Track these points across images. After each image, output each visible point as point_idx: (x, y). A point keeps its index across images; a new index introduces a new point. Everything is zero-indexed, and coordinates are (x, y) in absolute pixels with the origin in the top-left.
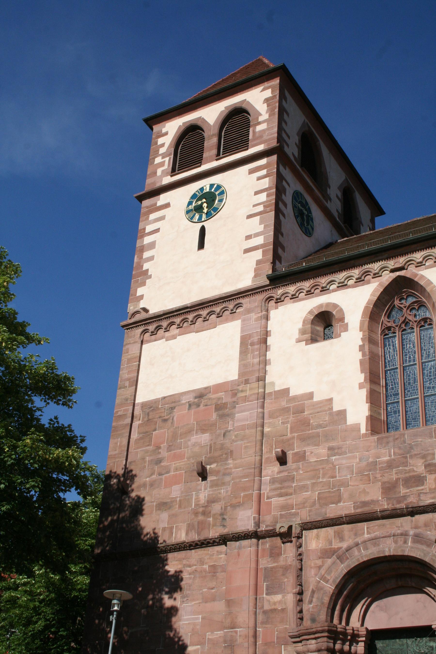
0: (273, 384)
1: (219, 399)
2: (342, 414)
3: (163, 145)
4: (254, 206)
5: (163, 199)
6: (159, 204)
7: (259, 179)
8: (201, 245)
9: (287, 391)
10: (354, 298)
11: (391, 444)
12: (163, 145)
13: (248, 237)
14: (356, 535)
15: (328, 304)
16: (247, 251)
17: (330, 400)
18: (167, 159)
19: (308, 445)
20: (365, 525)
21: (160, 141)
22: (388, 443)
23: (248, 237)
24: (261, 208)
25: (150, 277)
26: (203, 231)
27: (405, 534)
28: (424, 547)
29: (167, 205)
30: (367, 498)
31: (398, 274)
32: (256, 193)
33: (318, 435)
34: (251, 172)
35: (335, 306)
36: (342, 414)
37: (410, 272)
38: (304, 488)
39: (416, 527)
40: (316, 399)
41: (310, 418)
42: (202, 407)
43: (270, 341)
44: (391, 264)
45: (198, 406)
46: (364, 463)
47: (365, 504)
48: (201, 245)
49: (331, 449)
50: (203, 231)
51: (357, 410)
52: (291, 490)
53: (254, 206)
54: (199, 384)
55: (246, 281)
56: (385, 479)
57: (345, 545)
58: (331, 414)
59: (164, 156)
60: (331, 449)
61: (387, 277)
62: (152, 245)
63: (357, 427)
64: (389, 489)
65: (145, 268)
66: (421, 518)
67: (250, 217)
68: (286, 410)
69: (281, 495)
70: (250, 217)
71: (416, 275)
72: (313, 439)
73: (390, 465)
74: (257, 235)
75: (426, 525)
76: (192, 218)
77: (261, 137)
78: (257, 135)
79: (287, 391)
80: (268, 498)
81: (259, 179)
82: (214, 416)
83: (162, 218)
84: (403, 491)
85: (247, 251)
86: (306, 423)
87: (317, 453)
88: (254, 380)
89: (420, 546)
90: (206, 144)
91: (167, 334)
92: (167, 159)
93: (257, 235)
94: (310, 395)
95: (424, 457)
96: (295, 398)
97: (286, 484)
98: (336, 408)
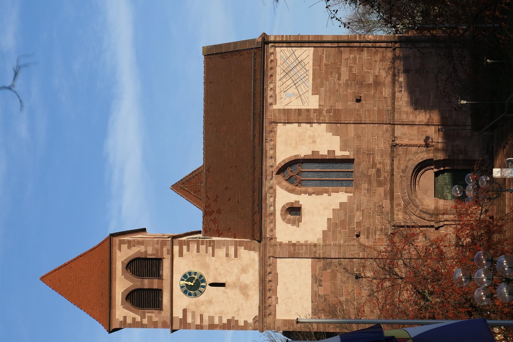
0: (318, 239)
1: (320, 269)
2: (341, 204)
3: (134, 319)
4: (207, 252)
5: (178, 314)
6: (181, 316)
8: (223, 285)
9: (324, 232)
10: (282, 197)
11: (361, 182)
12: (134, 319)
14: (399, 198)
15: (282, 211)
18: (147, 314)
19: (354, 220)
20: (395, 194)
21: (129, 321)
22: (359, 184)
23: (227, 255)
24: (210, 249)
25: (233, 317)
26: (212, 285)
27: (401, 177)
28: (408, 169)
30: (383, 194)
31: (274, 175)
33: (350, 216)
34: (181, 254)
35: (284, 206)
36: (341, 204)
37: (275, 170)
38: (374, 222)
39: (399, 172)
40: (331, 217)
42: (323, 279)
43: (294, 242)
44: (269, 177)
45: (321, 280)
46: (367, 195)
47: (385, 195)
48: (223, 285)
49: (357, 210)
50: (212, 285)
51: (341, 197)
52: (374, 229)
53: (207, 252)
54: (309, 280)
55: (255, 256)
56: (376, 185)
57: (402, 203)
58: (340, 209)
60: (357, 210)
62: (211, 318)
63: (349, 198)
64: (380, 184)
65: (226, 322)
66: (396, 170)
67: (213, 255)
68: (334, 231)
69: (375, 234)
70: (213, 255)
71: (278, 166)
72: (351, 218)
73: (370, 183)
74: (227, 250)
75: (398, 168)
76: (201, 292)
77: (157, 250)
78: (154, 252)
79: (324, 232)
80: (376, 240)
81: (188, 250)
82: (329, 271)
83: (193, 313)
84: (382, 178)
85: (236, 256)
86: (343, 223)
87: (358, 217)
88: (315, 248)
89: (407, 171)
91: (274, 303)
92: (147, 314)
93: (227, 250)
94: (329, 220)
95: (368, 169)
96: (328, 227)
97: (371, 231)
98: (338, 207)
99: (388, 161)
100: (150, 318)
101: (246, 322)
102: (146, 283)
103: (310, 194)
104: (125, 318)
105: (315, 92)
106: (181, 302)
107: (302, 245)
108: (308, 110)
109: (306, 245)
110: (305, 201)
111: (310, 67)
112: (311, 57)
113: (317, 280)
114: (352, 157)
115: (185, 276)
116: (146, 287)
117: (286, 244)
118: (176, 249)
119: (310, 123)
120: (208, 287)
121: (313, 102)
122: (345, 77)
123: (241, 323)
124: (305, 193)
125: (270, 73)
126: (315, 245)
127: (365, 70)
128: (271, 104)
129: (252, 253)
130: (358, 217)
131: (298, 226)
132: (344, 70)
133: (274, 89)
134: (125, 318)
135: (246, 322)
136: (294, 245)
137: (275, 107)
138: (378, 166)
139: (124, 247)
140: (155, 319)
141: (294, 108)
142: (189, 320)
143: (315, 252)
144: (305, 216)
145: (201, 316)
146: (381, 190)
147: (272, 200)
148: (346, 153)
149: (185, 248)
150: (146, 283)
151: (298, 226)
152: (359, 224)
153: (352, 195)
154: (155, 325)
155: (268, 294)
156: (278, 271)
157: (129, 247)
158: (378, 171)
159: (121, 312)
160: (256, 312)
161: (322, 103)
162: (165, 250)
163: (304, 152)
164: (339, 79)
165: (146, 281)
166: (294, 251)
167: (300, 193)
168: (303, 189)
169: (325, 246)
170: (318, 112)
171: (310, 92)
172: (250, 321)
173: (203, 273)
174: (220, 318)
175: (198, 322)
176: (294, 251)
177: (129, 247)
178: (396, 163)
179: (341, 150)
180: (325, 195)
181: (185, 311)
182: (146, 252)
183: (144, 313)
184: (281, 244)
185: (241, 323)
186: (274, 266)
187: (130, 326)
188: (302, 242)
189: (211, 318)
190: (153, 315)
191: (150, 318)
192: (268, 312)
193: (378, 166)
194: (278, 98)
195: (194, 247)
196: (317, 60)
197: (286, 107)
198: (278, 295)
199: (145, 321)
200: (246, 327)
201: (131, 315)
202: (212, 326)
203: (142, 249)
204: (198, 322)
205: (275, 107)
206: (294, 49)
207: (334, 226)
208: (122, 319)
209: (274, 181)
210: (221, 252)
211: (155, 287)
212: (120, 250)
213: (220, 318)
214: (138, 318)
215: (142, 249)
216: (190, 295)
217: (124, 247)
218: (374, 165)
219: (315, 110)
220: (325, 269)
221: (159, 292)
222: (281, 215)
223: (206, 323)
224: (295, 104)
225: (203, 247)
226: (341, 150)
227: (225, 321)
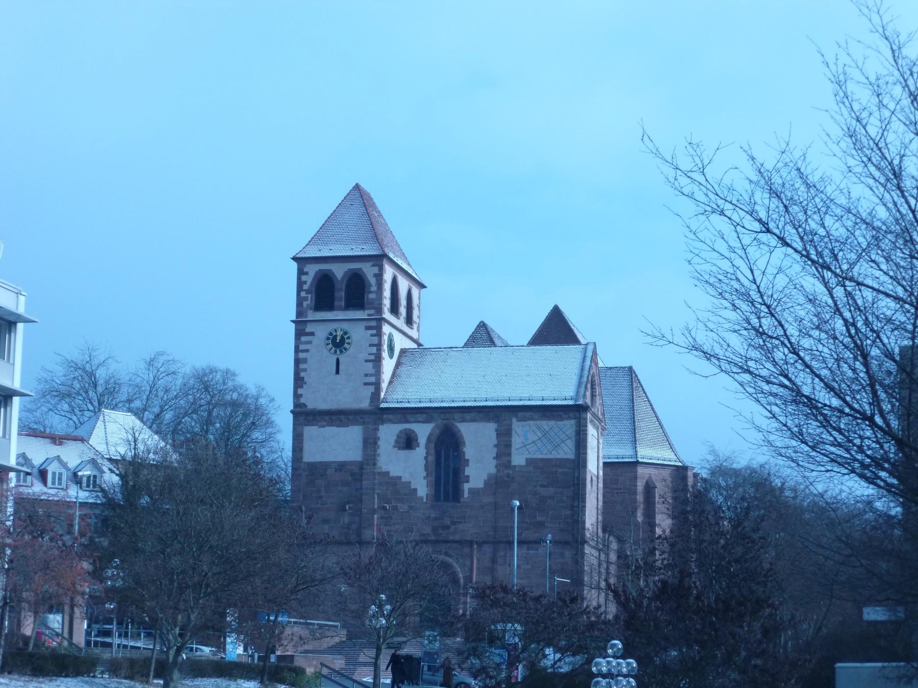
0: (381, 467)
3: (305, 282)
7: (372, 335)
8: (337, 372)
9: (388, 473)
10: (423, 431)
12: (305, 282)
13: (366, 375)
15: (410, 430)
16: (366, 384)
17: (410, 482)
18: (309, 296)
21: (304, 278)
23: (366, 375)
24: (373, 357)
26: (338, 360)
29: (312, 334)
32: (371, 345)
34: (368, 328)
35: (413, 432)
36: (415, 490)
41: (397, 488)
43: (380, 443)
44: (443, 416)
47: (424, 535)
48: (337, 372)
49: (410, 507)
50: (338, 360)
51: (422, 489)
54: (341, 459)
59: (307, 292)
60: (410, 507)
61: (439, 422)
62: (305, 361)
63: (422, 498)
64: (435, 529)
66: (449, 545)
67: (366, 361)
70: (366, 361)
73: (436, 519)
74: (371, 375)
79: (388, 473)
81: (372, 335)
82: (350, 479)
83: (310, 343)
84: (441, 531)
85: (366, 384)
87: (403, 507)
90: (336, 294)
92: (309, 296)
94: (400, 478)
96: (392, 477)
98: (412, 487)
99: (457, 538)
100: (306, 299)
101: (301, 396)
102: (340, 294)
103: (426, 458)
104: (307, 274)
105: (530, 461)
106: (321, 332)
107: (375, 451)
108: (510, 454)
109: (375, 455)
110: (420, 452)
111: (555, 455)
112: (565, 457)
113: (341, 466)
114: (462, 500)
115: (346, 333)
116: (336, 294)
117: (376, 434)
118: (374, 324)
119: (497, 457)
120: (335, 357)
121: (518, 459)
122: (543, 492)
123: (300, 391)
124: (427, 453)
125: (547, 414)
126: (375, 464)
127: (551, 513)
128: (517, 417)
129: (368, 401)
130: (403, 507)
131: (394, 447)
132: (551, 490)
133: (531, 419)
134: (307, 274)
135: (301, 396)
136: (376, 443)
137: (514, 420)
138: (453, 527)
139: (376, 270)
140: (305, 304)
141: (513, 440)
142: (303, 339)
143: (368, 464)
144: (404, 453)
145: (307, 351)
146: (428, 530)
147: (420, 419)
148: (466, 495)
149: (374, 332)
150: (340, 294)
151: (394, 447)
152: (395, 508)
153: (425, 500)
154: (299, 304)
155: (327, 418)
156: (350, 428)
157: (376, 275)
158: (448, 527)
159: (312, 270)
160: (310, 406)
161: (517, 469)
162: (372, 312)
163: (469, 451)
164: (542, 486)
165: (343, 294)
166: (370, 443)
167: (427, 447)
168: (432, 451)
169: (374, 474)
170: (508, 465)
171: (529, 456)
172: (302, 400)
173: (349, 352)
174: (305, 370)
175: (302, 347)
176: (370, 443)
177: (376, 275)
178: (455, 545)
179: (470, 489)
180: (425, 474)
181: (312, 334)
182: (371, 292)
183: (311, 293)
184: (377, 429)
185: (300, 391)
186: (355, 423)
187: (299, 278)
188: (379, 451)
189: (305, 361)
190: (309, 302)
191: (306, 299)
192: (310, 418)
193: (453, 527)
194: (524, 423)
195: (375, 340)
196: (561, 462)
197: (513, 432)
198: (327, 428)
199: (303, 294)
200: (297, 396)
201: (309, 279)
202: (297, 362)
203: (374, 288)
204: (302, 347)
205: (514, 420)
206: (573, 439)
207: (395, 482)
208: (305, 270)
209: (439, 422)
210: (369, 368)
211: (336, 303)
212: (373, 266)
213: (305, 370)
214: (306, 287)
215: (374, 288)
216: (328, 339)
217: (376, 270)
218: (454, 523)
219: (509, 462)
220: (352, 474)
221: (330, 307)
222: (406, 429)
223: (301, 355)
224: (516, 441)
225: (374, 350)
226: (470, 489)
227: (302, 374)
